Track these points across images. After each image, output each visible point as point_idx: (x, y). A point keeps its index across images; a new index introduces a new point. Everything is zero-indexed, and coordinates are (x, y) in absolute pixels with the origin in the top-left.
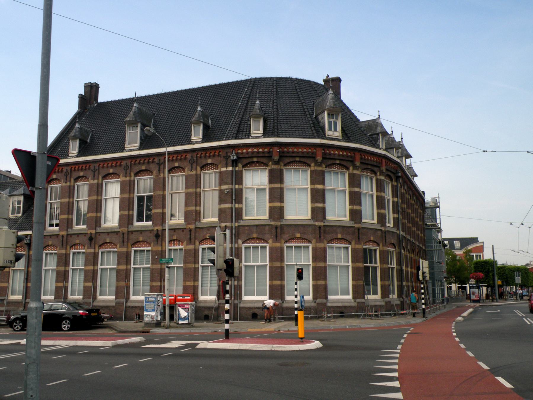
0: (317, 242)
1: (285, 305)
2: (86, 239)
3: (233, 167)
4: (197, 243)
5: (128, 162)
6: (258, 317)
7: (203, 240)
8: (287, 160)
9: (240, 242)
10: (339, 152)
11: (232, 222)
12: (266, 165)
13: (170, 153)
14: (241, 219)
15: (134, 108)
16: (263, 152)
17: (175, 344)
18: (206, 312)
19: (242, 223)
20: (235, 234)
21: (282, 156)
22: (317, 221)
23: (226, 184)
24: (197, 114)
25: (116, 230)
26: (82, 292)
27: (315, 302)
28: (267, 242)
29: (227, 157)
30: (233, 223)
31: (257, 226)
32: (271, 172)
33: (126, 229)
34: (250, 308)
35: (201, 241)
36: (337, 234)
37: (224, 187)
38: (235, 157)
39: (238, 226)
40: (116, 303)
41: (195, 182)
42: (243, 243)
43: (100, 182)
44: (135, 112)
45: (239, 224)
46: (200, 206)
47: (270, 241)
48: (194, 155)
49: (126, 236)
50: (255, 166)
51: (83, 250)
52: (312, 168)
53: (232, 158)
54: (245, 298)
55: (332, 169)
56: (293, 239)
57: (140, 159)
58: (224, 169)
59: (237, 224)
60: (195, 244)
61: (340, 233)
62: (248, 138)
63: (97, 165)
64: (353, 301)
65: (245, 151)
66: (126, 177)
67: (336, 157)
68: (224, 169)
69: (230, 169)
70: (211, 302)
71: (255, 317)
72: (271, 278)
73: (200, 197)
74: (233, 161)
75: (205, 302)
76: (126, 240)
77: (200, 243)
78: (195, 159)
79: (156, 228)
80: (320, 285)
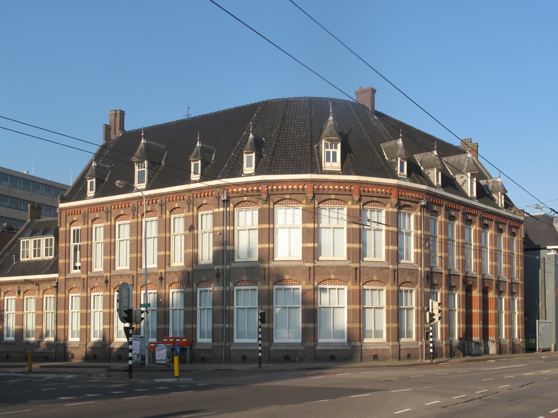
0: (306, 284)
1: (272, 348)
2: (80, 284)
3: (224, 207)
4: (195, 286)
5: (135, 202)
6: (248, 359)
7: (200, 282)
8: (276, 199)
9: (231, 284)
10: (334, 187)
11: (223, 265)
12: (256, 203)
13: (147, 197)
14: (233, 261)
15: (141, 145)
16: (238, 192)
17: (70, 376)
18: (203, 355)
19: (233, 265)
20: (226, 277)
21: (269, 196)
22: (307, 262)
23: (218, 226)
24: (195, 150)
25: (127, 273)
26: (79, 335)
27: (304, 345)
28: (256, 285)
29: (218, 198)
30: (224, 266)
31: (247, 268)
32: (261, 211)
33: (135, 272)
34: (240, 351)
35: (198, 284)
36: (329, 274)
37: (217, 229)
38: (225, 198)
39: (230, 269)
40: (103, 345)
41: (165, 226)
42: (235, 285)
43: (113, 223)
44: (142, 149)
45: (231, 267)
46: (197, 248)
47: (259, 284)
48: (191, 194)
49: (135, 278)
50: (247, 206)
51: (79, 294)
52: (304, 206)
53: (222, 198)
54: (236, 340)
55: (327, 205)
56: (329, 280)
57: (156, 198)
58: (216, 210)
59: (228, 267)
60: (193, 287)
61: (333, 274)
62: (240, 176)
63: (109, 206)
64: (347, 344)
65: (245, 189)
66: (134, 218)
67: (330, 192)
68: (216, 210)
69: (221, 209)
70: (208, 344)
71: (244, 359)
72: (304, 321)
73: (197, 238)
74: (224, 201)
75: (202, 344)
76: (135, 283)
77: (197, 285)
78: (192, 199)
79: (160, 271)
80: (309, 328)
